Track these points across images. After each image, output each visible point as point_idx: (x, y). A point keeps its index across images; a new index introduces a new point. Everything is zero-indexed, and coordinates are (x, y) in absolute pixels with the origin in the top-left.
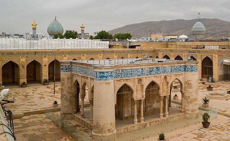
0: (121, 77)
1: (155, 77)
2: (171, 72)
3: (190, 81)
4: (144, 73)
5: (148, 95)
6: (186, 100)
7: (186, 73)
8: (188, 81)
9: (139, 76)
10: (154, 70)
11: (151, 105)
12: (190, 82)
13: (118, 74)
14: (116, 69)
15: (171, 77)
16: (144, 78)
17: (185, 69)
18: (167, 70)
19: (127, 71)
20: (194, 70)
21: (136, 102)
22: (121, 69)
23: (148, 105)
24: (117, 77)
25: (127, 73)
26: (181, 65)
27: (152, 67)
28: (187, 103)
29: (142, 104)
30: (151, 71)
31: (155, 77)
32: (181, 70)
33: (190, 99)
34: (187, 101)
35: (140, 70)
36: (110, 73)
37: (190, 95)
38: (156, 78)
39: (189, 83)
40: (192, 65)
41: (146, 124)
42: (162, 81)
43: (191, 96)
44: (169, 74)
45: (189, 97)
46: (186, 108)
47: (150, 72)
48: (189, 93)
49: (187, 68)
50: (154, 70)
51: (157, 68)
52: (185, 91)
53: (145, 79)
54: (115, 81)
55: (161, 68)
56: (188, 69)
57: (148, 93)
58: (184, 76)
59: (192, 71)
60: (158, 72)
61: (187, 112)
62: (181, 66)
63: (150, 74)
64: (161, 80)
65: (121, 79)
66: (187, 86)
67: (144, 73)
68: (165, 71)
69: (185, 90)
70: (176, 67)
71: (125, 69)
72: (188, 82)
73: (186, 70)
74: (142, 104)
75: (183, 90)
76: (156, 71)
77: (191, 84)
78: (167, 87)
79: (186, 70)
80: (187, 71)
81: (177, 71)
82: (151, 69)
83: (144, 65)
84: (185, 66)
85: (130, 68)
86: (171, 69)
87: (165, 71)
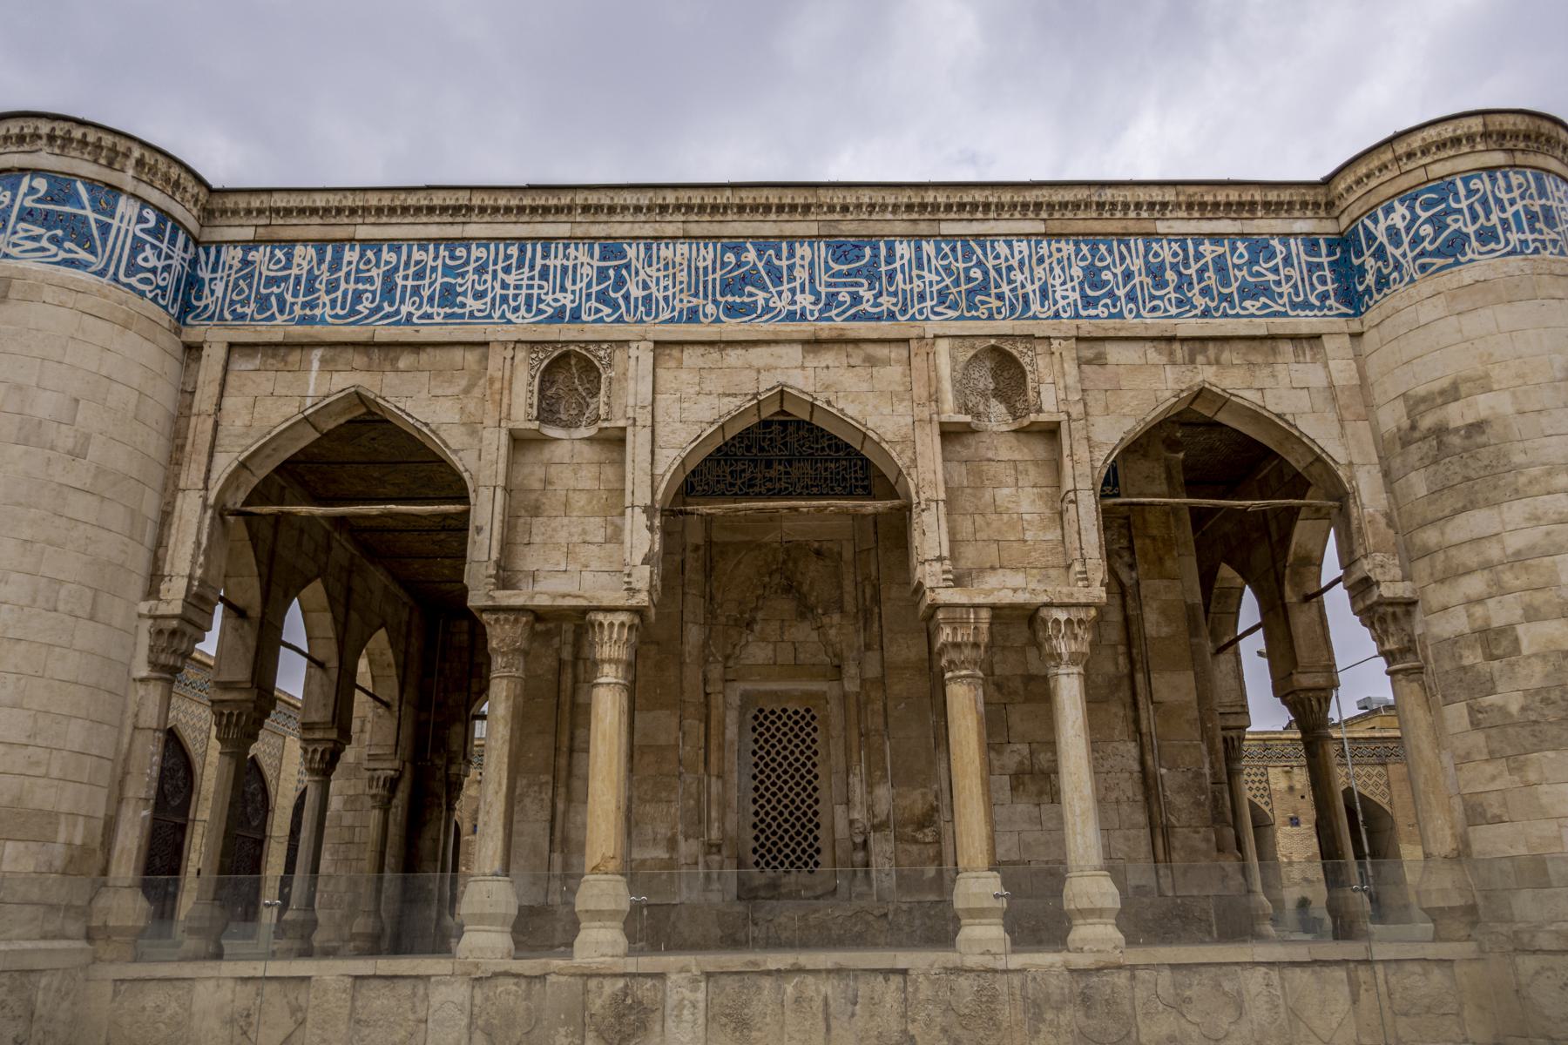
0: (304, 320)
1: (814, 344)
2: (1090, 302)
3: (1452, 393)
4: (641, 293)
5: (873, 671)
6: (1456, 715)
7: (1371, 317)
8: (1416, 405)
9: (558, 316)
10: (802, 275)
11: (919, 808)
12: (1457, 414)
13: (271, 281)
14: (248, 233)
15: (1099, 361)
16: (644, 354)
17: (1346, 273)
18: (1019, 277)
19: (386, 255)
20: (1486, 236)
21: (500, 636)
22: (315, 232)
23: (870, 808)
24: (243, 317)
25: (389, 277)
26: (1263, 225)
27: (768, 229)
28: (1492, 756)
29: (610, 675)
30: (744, 279)
31: (814, 344)
32: (1265, 290)
33: (1535, 675)
34: (1475, 725)
35: (586, 261)
36: (32, 190)
37: (1500, 613)
38: (829, 357)
39: (1440, 431)
40: (1438, 170)
41: (645, 989)
42: (935, 398)
43: (1532, 614)
44: (1067, 326)
45: (1493, 640)
46: (1489, 840)
47: (727, 287)
48: (1474, 585)
49: (1370, 263)
50: (802, 275)
51: (844, 249)
52: (1422, 568)
53: (647, 358)
54: (214, 357)
55: (903, 250)
56: (1380, 254)
57: (868, 647)
58: (1342, 369)
59: (1454, 247)
60: (857, 300)
61: (1526, 905)
62: (1259, 247)
63: (731, 311)
64: (920, 391)
65: (299, 332)
66: (1418, 484)
67: (636, 292)
68: (984, 288)
69: (1410, 555)
70: (1166, 252)
71: (363, 232)
72: (1427, 422)
73: (1370, 279)
74: (610, 675)
75: (1366, 567)
76: (825, 278)
77: (1478, 427)
78: (1059, 505)
79: (1370, 279)
80: (1382, 282)
81: (1201, 302)
82: (751, 255)
83: (630, 198)
84: (1345, 242)
85: (434, 231)
86: (1092, 276)
87: (984, 288)
